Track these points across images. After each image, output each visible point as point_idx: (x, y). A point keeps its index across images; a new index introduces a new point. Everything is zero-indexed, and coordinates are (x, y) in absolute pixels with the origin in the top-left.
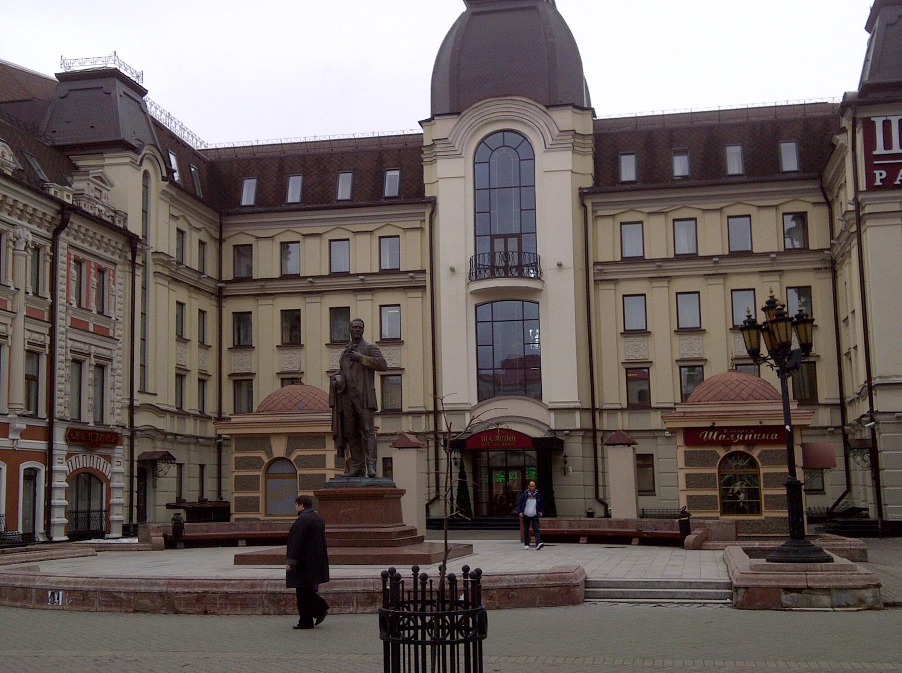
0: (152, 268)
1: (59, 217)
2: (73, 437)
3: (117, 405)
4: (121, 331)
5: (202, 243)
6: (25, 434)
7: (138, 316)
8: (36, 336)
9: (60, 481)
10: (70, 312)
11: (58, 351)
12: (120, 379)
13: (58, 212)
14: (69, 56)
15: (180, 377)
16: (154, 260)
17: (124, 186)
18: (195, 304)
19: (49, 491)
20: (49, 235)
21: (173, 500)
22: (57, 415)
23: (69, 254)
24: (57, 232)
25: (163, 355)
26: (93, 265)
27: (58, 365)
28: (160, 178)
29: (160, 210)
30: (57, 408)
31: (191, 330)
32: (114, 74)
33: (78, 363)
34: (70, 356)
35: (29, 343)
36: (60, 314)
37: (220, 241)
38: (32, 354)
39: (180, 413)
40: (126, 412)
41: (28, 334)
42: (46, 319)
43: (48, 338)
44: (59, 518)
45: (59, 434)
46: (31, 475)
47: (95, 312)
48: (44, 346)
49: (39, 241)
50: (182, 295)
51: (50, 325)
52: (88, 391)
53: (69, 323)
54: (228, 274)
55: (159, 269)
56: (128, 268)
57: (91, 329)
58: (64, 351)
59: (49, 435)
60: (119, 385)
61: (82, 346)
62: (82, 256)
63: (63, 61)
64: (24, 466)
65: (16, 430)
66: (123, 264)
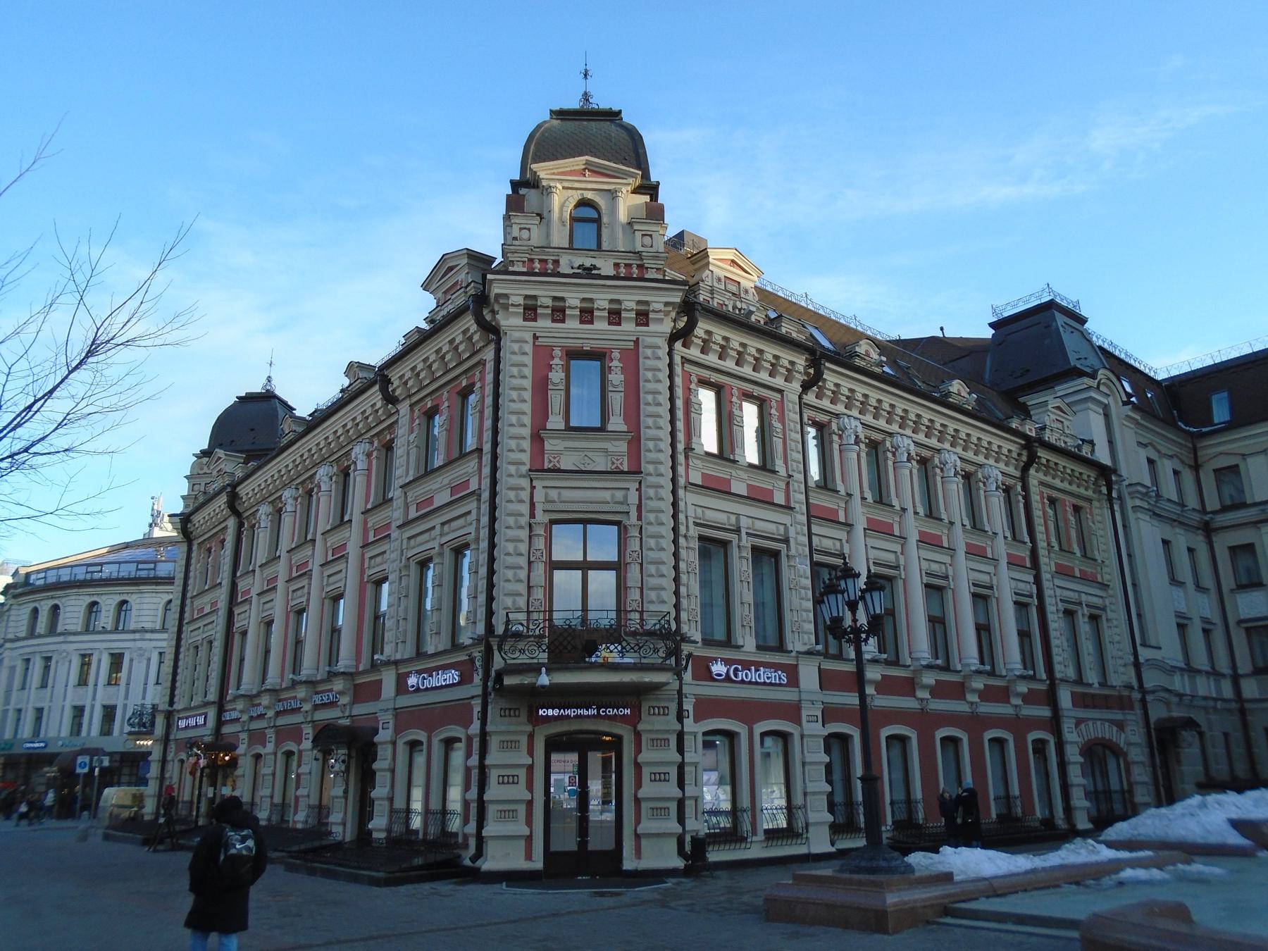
0: (1130, 503)
1: (1025, 453)
2: (1081, 701)
3: (1120, 662)
4: (1110, 574)
5: (1176, 473)
7: (1126, 558)
8: (1021, 585)
9: (1074, 755)
11: (1048, 600)
12: (1117, 631)
13: (1023, 447)
14: (999, 302)
15: (1181, 627)
17: (1079, 419)
18: (1181, 540)
19: (1063, 765)
20: (1018, 474)
21: (1202, 778)
22: (1058, 675)
23: (1042, 494)
24: (1025, 470)
25: (1163, 602)
27: (1050, 617)
30: (1057, 668)
31: (1185, 573)
32: (1051, 306)
33: (1069, 614)
34: (1061, 606)
36: (1043, 560)
37: (1196, 468)
38: (1021, 606)
39: (1190, 670)
40: (1132, 672)
42: (1028, 565)
43: (1034, 587)
44: (1079, 800)
45: (1065, 698)
46: (1040, 746)
47: (1078, 554)
48: (1031, 596)
49: (1010, 481)
52: (1087, 647)
53: (1054, 569)
54: (1212, 503)
55: (1138, 503)
56: (1106, 505)
57: (1077, 574)
59: (1051, 698)
60: (1117, 638)
62: (1055, 494)
63: (994, 312)
66: (1099, 501)
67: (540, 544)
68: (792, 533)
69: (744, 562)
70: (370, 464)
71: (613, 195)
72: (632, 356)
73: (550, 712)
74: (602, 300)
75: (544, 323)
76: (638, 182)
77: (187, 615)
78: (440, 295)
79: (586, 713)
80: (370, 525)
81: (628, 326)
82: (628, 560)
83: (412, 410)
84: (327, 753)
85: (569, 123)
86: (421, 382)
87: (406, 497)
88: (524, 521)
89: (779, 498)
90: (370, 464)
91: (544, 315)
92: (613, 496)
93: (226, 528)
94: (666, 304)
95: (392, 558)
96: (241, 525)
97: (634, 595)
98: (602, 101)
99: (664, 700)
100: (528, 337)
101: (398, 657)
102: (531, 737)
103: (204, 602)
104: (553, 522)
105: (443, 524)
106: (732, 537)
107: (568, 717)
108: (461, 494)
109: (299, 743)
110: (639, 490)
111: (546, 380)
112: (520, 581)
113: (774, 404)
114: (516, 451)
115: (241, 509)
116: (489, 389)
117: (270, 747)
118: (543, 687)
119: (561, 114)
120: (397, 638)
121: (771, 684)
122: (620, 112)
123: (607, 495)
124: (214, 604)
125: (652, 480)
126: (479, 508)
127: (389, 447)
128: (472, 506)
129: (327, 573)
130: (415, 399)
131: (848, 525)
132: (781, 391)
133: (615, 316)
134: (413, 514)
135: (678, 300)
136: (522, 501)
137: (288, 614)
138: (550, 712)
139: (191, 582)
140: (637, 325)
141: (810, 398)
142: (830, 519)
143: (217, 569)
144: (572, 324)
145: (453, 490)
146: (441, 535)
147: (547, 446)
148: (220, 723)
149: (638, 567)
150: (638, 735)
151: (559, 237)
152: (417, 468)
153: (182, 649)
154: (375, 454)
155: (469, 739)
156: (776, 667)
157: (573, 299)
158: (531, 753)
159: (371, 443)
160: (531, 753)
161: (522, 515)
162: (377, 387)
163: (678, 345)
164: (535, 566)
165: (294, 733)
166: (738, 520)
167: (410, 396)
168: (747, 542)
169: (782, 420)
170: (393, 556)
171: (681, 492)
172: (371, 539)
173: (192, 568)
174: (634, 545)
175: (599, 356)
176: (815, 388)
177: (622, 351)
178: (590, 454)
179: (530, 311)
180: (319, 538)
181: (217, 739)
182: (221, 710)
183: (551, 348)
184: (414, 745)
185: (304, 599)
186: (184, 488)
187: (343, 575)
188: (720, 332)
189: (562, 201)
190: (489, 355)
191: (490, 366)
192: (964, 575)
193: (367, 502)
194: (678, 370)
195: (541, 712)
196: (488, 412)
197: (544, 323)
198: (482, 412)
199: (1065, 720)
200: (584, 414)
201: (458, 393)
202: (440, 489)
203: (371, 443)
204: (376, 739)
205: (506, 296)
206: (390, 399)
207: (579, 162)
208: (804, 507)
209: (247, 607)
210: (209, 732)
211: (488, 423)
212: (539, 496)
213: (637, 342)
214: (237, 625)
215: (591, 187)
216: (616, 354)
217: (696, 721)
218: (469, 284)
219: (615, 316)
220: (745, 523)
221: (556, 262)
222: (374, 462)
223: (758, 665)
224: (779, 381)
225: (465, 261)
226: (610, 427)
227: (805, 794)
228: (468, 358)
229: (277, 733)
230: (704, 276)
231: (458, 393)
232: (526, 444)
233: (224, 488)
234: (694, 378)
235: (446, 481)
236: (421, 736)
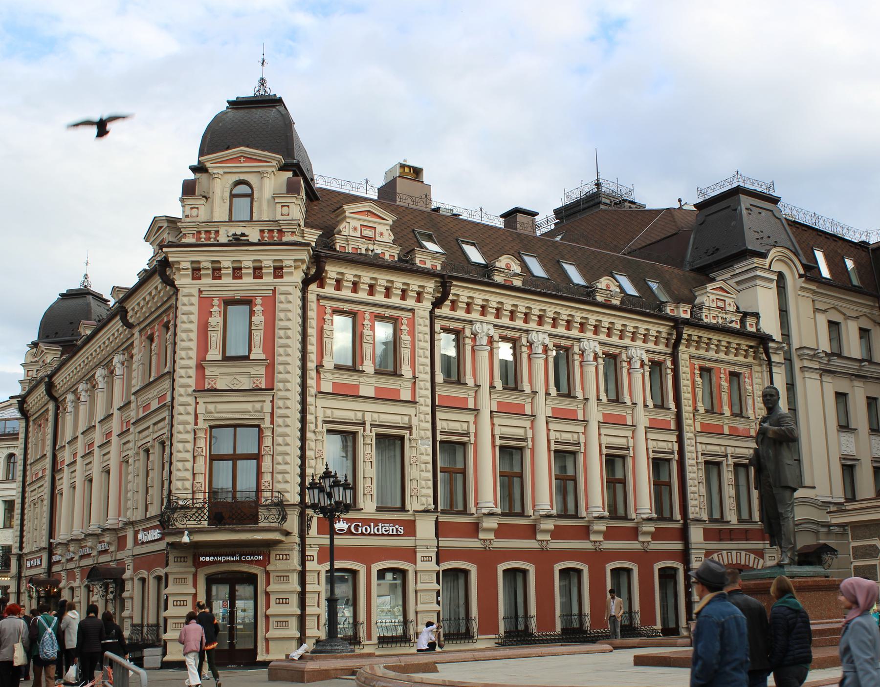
1: (674, 332)
2: (709, 535)
6: (657, 535)
8: (661, 444)
10: (697, 417)
11: (688, 455)
16: (799, 356)
22: (691, 516)
26: (722, 371)
28: (797, 276)
29: (801, 306)
30: (691, 510)
34: (701, 459)
35: (654, 452)
36: (687, 421)
38: (658, 464)
42: (673, 427)
45: (696, 534)
48: (672, 453)
49: (657, 358)
50: (843, 385)
51: (677, 433)
53: (698, 429)
55: (806, 363)
56: (765, 368)
57: (726, 431)
58: (694, 455)
61: (717, 448)
64: (657, 566)
67: (201, 443)
68: (414, 422)
72: (271, 301)
73: (208, 559)
74: (247, 260)
75: (207, 281)
77: (28, 478)
79: (232, 559)
81: (268, 279)
82: (263, 453)
83: (141, 335)
88: (190, 427)
89: (406, 395)
91: (207, 275)
92: (254, 407)
93: (47, 410)
94: (296, 260)
97: (267, 477)
99: (285, 550)
100: (195, 291)
102: (195, 576)
104: (211, 427)
105: (154, 424)
106: (360, 429)
107: (220, 562)
110: (272, 402)
111: (206, 324)
112: (187, 470)
114: (186, 377)
118: (185, 543)
119: (237, 104)
121: (388, 535)
123: (249, 406)
125: (280, 394)
130: (142, 326)
131: (476, 410)
132: (412, 311)
134: (141, 415)
136: (188, 413)
138: (208, 559)
141: (445, 310)
143: (43, 440)
147: (207, 373)
148: (50, 564)
149: (270, 458)
150: (268, 574)
151: (220, 213)
153: (26, 506)
156: (394, 522)
157: (226, 262)
158: (195, 585)
160: (195, 585)
161: (189, 423)
163: (313, 287)
164: (197, 459)
166: (363, 416)
169: (412, 333)
171: (310, 400)
174: (267, 442)
175: (248, 302)
176: (448, 303)
178: (237, 377)
179: (196, 272)
181: (49, 576)
182: (51, 554)
183: (212, 299)
184: (143, 580)
188: (350, 273)
194: (313, 305)
195: (201, 559)
197: (207, 281)
199: (693, 551)
200: (237, 348)
202: (153, 398)
204: (125, 576)
205: (178, 263)
212: (201, 409)
213: (274, 290)
216: (259, 301)
219: (258, 272)
220: (368, 418)
223: (376, 522)
224: (410, 303)
225: (165, 225)
227: (417, 613)
232: (192, 372)
234: (329, 310)
236: (144, 574)
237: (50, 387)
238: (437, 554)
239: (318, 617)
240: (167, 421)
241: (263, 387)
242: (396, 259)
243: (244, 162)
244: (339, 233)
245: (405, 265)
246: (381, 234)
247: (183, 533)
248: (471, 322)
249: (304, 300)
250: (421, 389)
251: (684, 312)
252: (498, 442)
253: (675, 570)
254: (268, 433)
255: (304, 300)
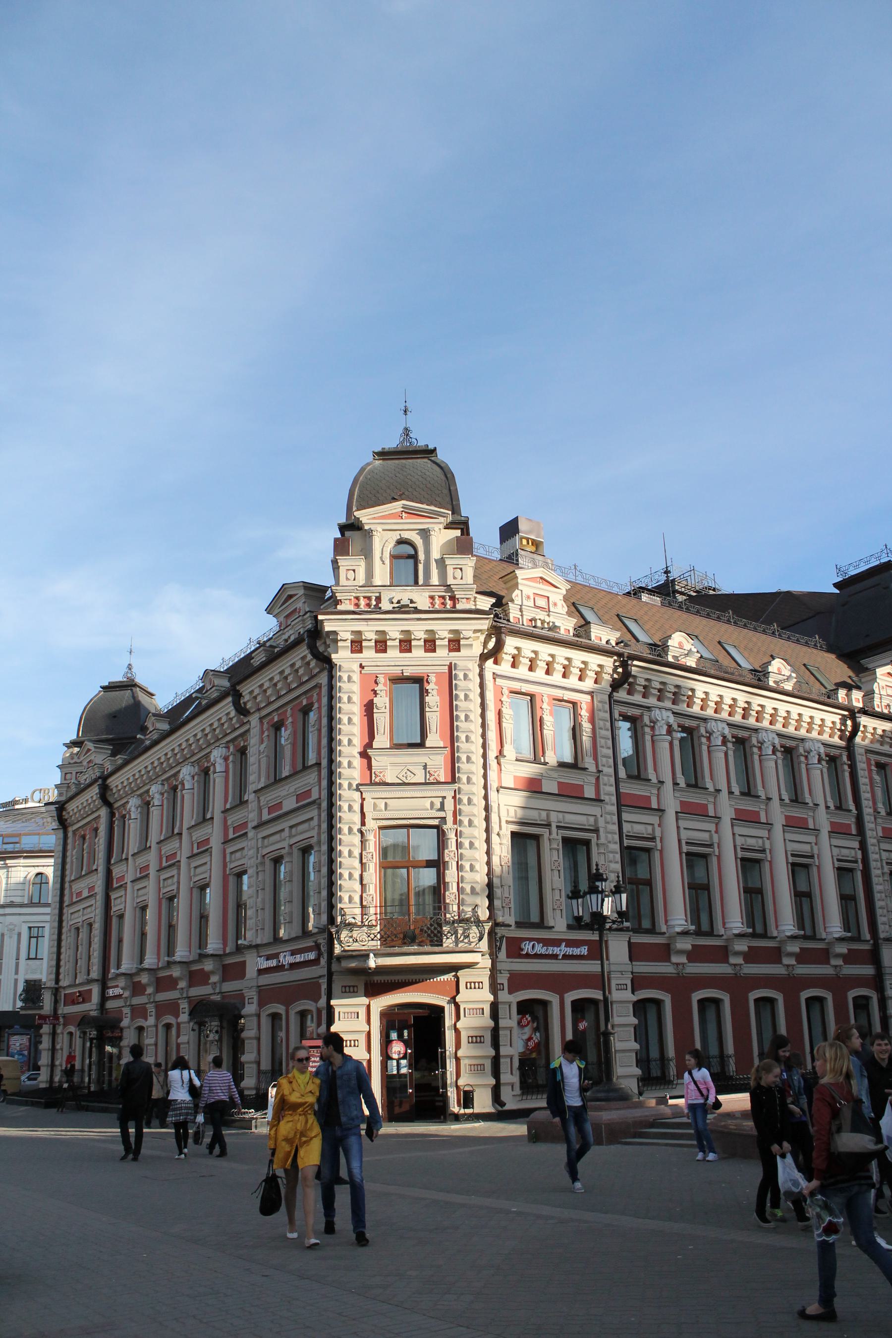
8: (845, 852)
10: (879, 820)
11: (873, 864)
22: (882, 935)
23: (868, 760)
27: (875, 880)
36: (869, 824)
38: (843, 872)
41: (836, 851)
42: (854, 832)
46: (862, 1004)
48: (856, 862)
49: (833, 752)
51: (859, 838)
58: (879, 864)
62: (883, 760)
64: (852, 994)
65: (838, 956)
68: (601, 823)
69: (555, 853)
70: (227, 766)
71: (425, 534)
75: (369, 654)
76: (450, 519)
78: (282, 619)
80: (229, 822)
81: (442, 652)
84: (201, 1024)
85: (389, 462)
86: (268, 698)
87: (259, 801)
89: (589, 792)
90: (227, 766)
91: (368, 647)
94: (476, 631)
95: (249, 854)
96: (112, 814)
98: (422, 440)
100: (356, 667)
101: (259, 942)
103: (82, 886)
105: (291, 827)
106: (544, 831)
108: (305, 802)
109: (177, 1016)
113: (584, 706)
114: (350, 769)
115: (111, 800)
116: (324, 710)
117: (151, 1021)
119: (383, 455)
120: (257, 925)
122: (435, 449)
124: (91, 889)
126: (320, 815)
127: (243, 752)
128: (314, 813)
129: (193, 865)
130: (264, 713)
133: (430, 645)
134: (266, 816)
135: (485, 627)
137: (160, 901)
139: (68, 867)
140: (450, 650)
141: (622, 695)
142: (643, 805)
144: (393, 653)
145: (299, 797)
146: (291, 836)
148: (104, 998)
152: (268, 777)
154: (231, 758)
155: (319, 1011)
159: (228, 748)
162: (230, 699)
163: (490, 663)
165: (172, 1008)
166: (548, 816)
167: (259, 710)
168: (557, 836)
170: (251, 853)
171: (493, 795)
172: (231, 836)
173: (69, 854)
175: (419, 681)
176: (626, 686)
177: (438, 675)
179: (357, 645)
180: (185, 832)
181: (102, 1013)
182: (104, 987)
184: (275, 1017)
185: (175, 887)
186: (56, 777)
187: (207, 867)
188: (528, 647)
189: (383, 543)
190: (323, 679)
191: (324, 690)
192: (780, 849)
193: (226, 801)
196: (324, 731)
197: (369, 654)
198: (320, 730)
199: (887, 977)
201: (300, 710)
202: (286, 797)
203: (228, 748)
206: (242, 711)
207: (397, 506)
208: (614, 799)
209: (123, 893)
210: (94, 1007)
211: (324, 741)
214: (114, 909)
215: (410, 530)
216: (433, 678)
217: (510, 992)
218: (306, 613)
219: (430, 645)
220: (554, 817)
221: (378, 599)
222: (231, 766)
223: (570, 943)
225: (301, 592)
226: (428, 743)
228: (307, 681)
229: (157, 1007)
230: (514, 596)
231: (300, 710)
233: (95, 781)
234: (505, 691)
235: (292, 790)
236: (280, 1009)
237: (105, 790)
238: (632, 981)
239: (511, 1059)
240: (315, 822)
241: (443, 780)
242: (572, 634)
243: (406, 518)
244: (512, 601)
245: (581, 641)
246: (555, 604)
247: (368, 956)
248: (649, 708)
249: (481, 675)
250: (605, 785)
251: (857, 699)
252: (685, 849)
253: (867, 998)
254: (451, 836)
255: (481, 675)
